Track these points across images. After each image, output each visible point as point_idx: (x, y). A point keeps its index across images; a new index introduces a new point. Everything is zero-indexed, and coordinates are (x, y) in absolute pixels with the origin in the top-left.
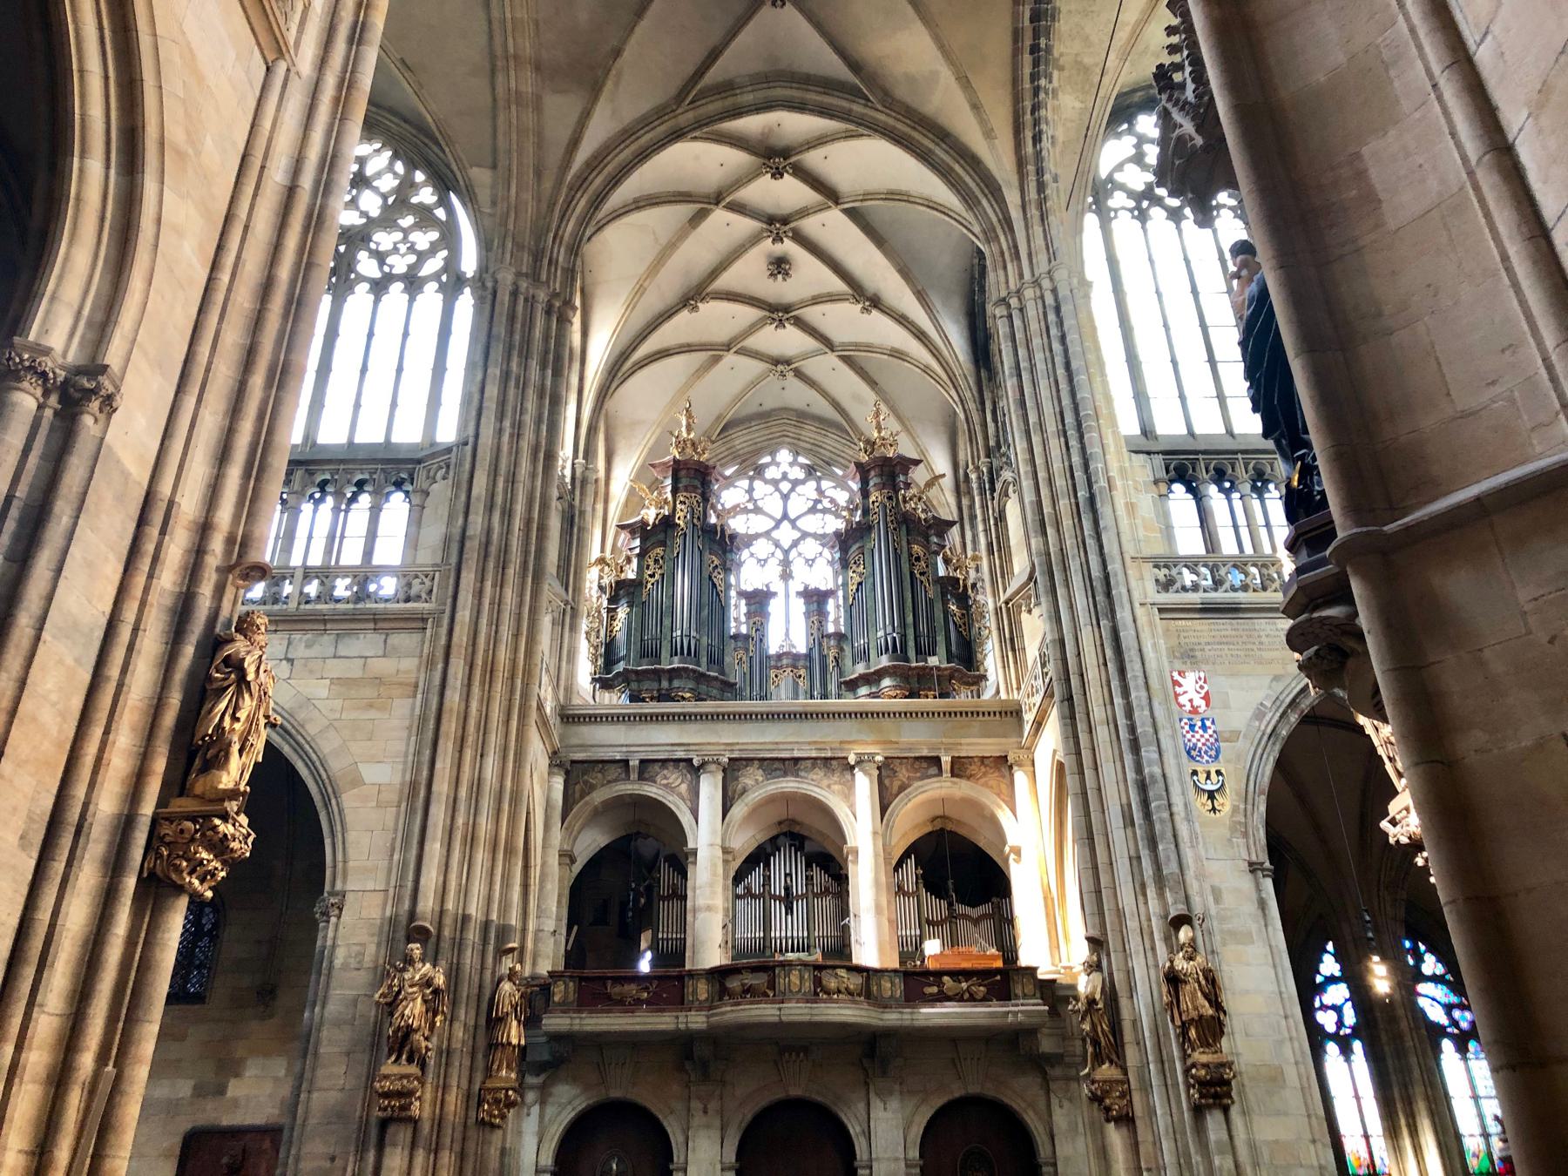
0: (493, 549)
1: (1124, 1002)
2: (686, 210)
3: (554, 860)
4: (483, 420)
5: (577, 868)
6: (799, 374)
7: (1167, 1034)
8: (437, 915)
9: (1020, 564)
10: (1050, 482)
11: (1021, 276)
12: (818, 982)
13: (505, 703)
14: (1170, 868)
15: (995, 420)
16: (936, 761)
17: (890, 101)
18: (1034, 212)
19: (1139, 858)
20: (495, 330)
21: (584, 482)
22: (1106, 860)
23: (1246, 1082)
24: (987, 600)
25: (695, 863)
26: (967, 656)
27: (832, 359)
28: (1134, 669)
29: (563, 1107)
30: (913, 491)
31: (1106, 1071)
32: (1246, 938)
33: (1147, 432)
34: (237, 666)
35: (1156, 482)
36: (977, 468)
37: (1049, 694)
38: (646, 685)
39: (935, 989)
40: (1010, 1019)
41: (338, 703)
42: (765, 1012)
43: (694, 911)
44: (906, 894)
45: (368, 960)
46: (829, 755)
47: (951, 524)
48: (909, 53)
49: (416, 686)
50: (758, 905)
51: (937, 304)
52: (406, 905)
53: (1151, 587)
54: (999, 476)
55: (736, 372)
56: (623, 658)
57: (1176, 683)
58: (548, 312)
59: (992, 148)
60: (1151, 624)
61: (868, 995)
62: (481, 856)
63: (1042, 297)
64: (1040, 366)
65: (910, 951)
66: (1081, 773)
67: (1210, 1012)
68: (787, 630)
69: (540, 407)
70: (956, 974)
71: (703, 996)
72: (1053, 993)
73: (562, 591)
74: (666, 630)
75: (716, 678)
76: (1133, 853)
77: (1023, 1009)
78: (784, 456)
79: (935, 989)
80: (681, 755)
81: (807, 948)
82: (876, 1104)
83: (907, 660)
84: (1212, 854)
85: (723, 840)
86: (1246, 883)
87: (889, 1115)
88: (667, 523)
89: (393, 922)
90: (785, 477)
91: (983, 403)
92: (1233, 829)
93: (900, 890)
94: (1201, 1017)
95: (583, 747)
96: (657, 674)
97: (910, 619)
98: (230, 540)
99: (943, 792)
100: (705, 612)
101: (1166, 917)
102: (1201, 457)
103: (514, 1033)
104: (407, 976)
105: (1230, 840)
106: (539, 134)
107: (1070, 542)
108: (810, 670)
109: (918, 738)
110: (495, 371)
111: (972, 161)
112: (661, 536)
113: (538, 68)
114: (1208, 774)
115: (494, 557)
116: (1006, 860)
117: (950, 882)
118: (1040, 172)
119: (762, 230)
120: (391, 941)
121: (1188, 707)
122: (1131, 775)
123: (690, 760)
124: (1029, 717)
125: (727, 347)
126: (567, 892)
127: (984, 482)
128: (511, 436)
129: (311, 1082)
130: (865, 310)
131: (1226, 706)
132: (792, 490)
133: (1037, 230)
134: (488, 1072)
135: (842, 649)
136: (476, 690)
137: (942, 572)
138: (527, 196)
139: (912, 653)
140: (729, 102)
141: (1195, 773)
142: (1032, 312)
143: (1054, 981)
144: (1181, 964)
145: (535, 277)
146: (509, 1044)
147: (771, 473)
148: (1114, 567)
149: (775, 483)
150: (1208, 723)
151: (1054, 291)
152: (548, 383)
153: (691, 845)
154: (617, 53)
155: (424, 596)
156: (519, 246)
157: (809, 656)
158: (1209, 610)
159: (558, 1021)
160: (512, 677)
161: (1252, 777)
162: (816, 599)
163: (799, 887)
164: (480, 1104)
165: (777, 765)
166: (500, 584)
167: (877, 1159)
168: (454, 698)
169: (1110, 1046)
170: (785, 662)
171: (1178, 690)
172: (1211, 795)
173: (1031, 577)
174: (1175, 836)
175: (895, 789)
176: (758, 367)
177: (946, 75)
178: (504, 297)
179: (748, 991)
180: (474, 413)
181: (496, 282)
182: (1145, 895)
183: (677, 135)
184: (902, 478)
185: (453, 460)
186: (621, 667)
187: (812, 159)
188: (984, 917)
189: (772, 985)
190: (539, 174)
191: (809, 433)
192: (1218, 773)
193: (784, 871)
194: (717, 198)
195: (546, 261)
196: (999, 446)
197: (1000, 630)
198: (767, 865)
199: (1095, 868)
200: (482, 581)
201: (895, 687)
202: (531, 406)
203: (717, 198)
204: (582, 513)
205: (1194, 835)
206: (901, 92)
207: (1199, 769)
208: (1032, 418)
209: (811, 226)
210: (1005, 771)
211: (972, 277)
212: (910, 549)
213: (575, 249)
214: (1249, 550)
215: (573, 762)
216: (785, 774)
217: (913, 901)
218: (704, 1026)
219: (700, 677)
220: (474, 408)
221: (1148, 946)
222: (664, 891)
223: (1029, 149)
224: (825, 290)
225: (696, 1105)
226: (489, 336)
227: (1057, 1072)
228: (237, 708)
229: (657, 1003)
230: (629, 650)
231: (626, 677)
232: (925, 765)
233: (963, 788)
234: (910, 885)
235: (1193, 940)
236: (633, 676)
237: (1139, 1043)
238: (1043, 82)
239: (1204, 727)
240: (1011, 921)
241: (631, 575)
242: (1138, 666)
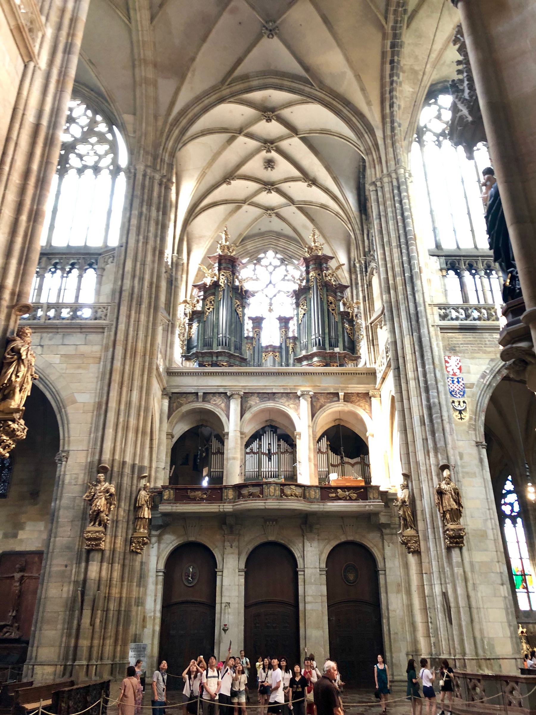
0: (135, 296)
1: (418, 502)
2: (225, 136)
3: (164, 437)
4: (130, 235)
5: (175, 440)
6: (278, 215)
7: (437, 517)
8: (111, 462)
9: (378, 305)
10: (393, 268)
11: (382, 172)
12: (282, 491)
13: (141, 367)
14: (441, 444)
15: (368, 239)
16: (337, 394)
17: (323, 86)
18: (389, 141)
19: (427, 439)
20: (135, 193)
21: (177, 265)
22: (412, 440)
23: (470, 537)
24: (362, 322)
25: (228, 439)
26: (352, 348)
27: (293, 208)
28: (428, 355)
29: (169, 544)
30: (330, 271)
31: (409, 532)
32: (474, 475)
33: (438, 246)
34: (17, 352)
35: (441, 270)
36: (359, 261)
37: (389, 366)
38: (206, 359)
39: (334, 495)
40: (367, 508)
41: (64, 366)
43: (227, 459)
44: (322, 453)
45: (80, 482)
46: (289, 391)
47: (347, 287)
48: (332, 62)
49: (100, 359)
50: (256, 456)
51: (343, 184)
52: (97, 457)
53: (437, 318)
54: (369, 265)
55: (249, 213)
56: (195, 347)
57: (446, 362)
58: (160, 184)
59: (370, 110)
60: (436, 335)
61: (305, 497)
62: (131, 435)
63: (392, 182)
64: (390, 215)
65: (323, 478)
66: (402, 401)
67: (456, 507)
68: (270, 336)
69: (157, 229)
70: (343, 488)
71: (231, 497)
72: (387, 498)
73: (166, 315)
74: (215, 334)
75: (238, 356)
76: (424, 437)
77: (373, 504)
78: (270, 254)
79: (334, 495)
80: (221, 390)
81: (277, 476)
82: (307, 544)
83: (325, 349)
84: (459, 438)
85: (241, 428)
86: (474, 451)
87: (313, 549)
88: (216, 285)
89: (91, 463)
90: (270, 264)
91: (363, 231)
92: (469, 427)
93: (320, 451)
94: (452, 509)
95: (178, 386)
96: (211, 354)
97: (327, 331)
98: (13, 294)
99: (340, 409)
100: (233, 326)
101: (438, 465)
102: (462, 258)
103: (146, 513)
104: (98, 488)
105: (468, 432)
106: (156, 100)
107: (401, 297)
108: (281, 353)
109: (329, 384)
110: (135, 212)
111: (361, 116)
112: (213, 291)
113: (155, 66)
114: (459, 402)
115: (135, 300)
116: (367, 438)
117: (342, 448)
118: (392, 122)
119: (262, 146)
120: (90, 473)
121: (451, 373)
122: (424, 403)
123: (226, 393)
124: (379, 376)
125: (244, 201)
126: (170, 451)
127: (362, 268)
128: (143, 243)
129: (56, 533)
130: (309, 185)
131: (469, 372)
132: (274, 270)
133: (390, 150)
134: (135, 530)
135: (295, 344)
136: (128, 361)
137: (342, 309)
138: (150, 129)
139: (327, 346)
140: (246, 85)
141: (453, 402)
142: (387, 189)
143: (387, 492)
144: (444, 486)
145: (154, 168)
146: (144, 518)
147: (264, 262)
148: (421, 309)
149: (267, 266)
150: (460, 380)
151: (397, 179)
152: (160, 218)
153: (226, 430)
154: (193, 59)
155: (103, 317)
156: (147, 153)
157: (280, 347)
158: (463, 329)
159: (167, 507)
160: (144, 355)
161: (479, 404)
162: (284, 321)
163: (274, 449)
164: (131, 544)
165: (266, 395)
166: (139, 312)
168: (118, 364)
169: (411, 521)
170: (269, 349)
171: (447, 365)
172: (460, 412)
173: (383, 312)
174: (443, 430)
175: (318, 407)
176: (258, 211)
177: (350, 74)
178: (140, 177)
179: (251, 495)
180: (125, 232)
181: (136, 169)
182: (429, 456)
183: (221, 100)
184: (325, 265)
185: (116, 255)
186: (194, 350)
187: (286, 113)
188: (357, 463)
189: (262, 492)
190: (156, 117)
191: (282, 243)
192: (464, 402)
193: (267, 442)
194: (240, 131)
195: (159, 160)
196: (370, 251)
197: (368, 336)
198: (260, 440)
199: (407, 444)
200: (130, 311)
201: (319, 361)
202: (152, 229)
203: (240, 131)
204: (176, 279)
205: (451, 429)
206: (328, 82)
207: (456, 400)
208: (385, 240)
209: (284, 145)
210: (368, 399)
211: (360, 171)
212: (327, 298)
213: (173, 155)
214: (482, 302)
215: (173, 393)
216: (269, 400)
217: (325, 456)
218: (231, 510)
219: (231, 356)
220: (126, 230)
221: (429, 478)
222: (214, 450)
223: (388, 111)
224: (290, 176)
225: (227, 544)
226: (133, 196)
227: (387, 531)
228: (18, 372)
229: (210, 500)
230: (198, 342)
231: (197, 355)
232: (332, 396)
233: (349, 407)
234: (324, 449)
235: (450, 475)
236: (200, 355)
237: (424, 520)
238: (395, 78)
239: (458, 382)
240: (369, 466)
241: (199, 307)
242: (429, 354)
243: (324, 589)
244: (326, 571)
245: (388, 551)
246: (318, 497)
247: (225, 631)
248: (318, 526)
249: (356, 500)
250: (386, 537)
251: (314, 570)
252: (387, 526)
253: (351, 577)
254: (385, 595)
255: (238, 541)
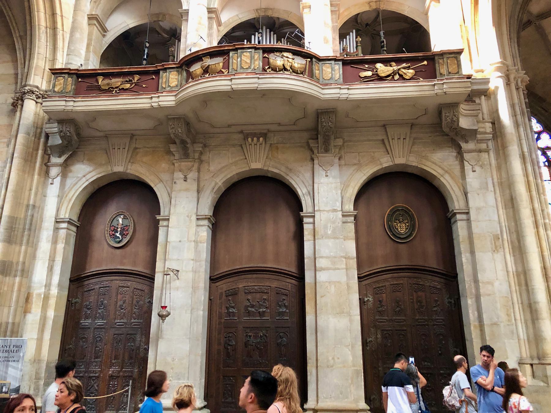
3: (84, 21)
5: (111, 37)
12: (266, 62)
25: (187, 20)
39: (369, 73)
42: (220, 84)
61: (311, 75)
79: (369, 73)
82: (320, 173)
87: (331, 180)
117: (382, 33)
153: (185, 7)
167: (319, 210)
189: (227, 66)
225: (179, 175)
234: (352, 49)
243: (351, 247)
244: (355, 217)
245: (473, 179)
246: (337, 76)
247: (162, 317)
248: (339, 142)
249: (411, 79)
250: (466, 156)
251: (331, 215)
252: (471, 135)
253: (402, 228)
254: (468, 255)
255: (199, 171)
